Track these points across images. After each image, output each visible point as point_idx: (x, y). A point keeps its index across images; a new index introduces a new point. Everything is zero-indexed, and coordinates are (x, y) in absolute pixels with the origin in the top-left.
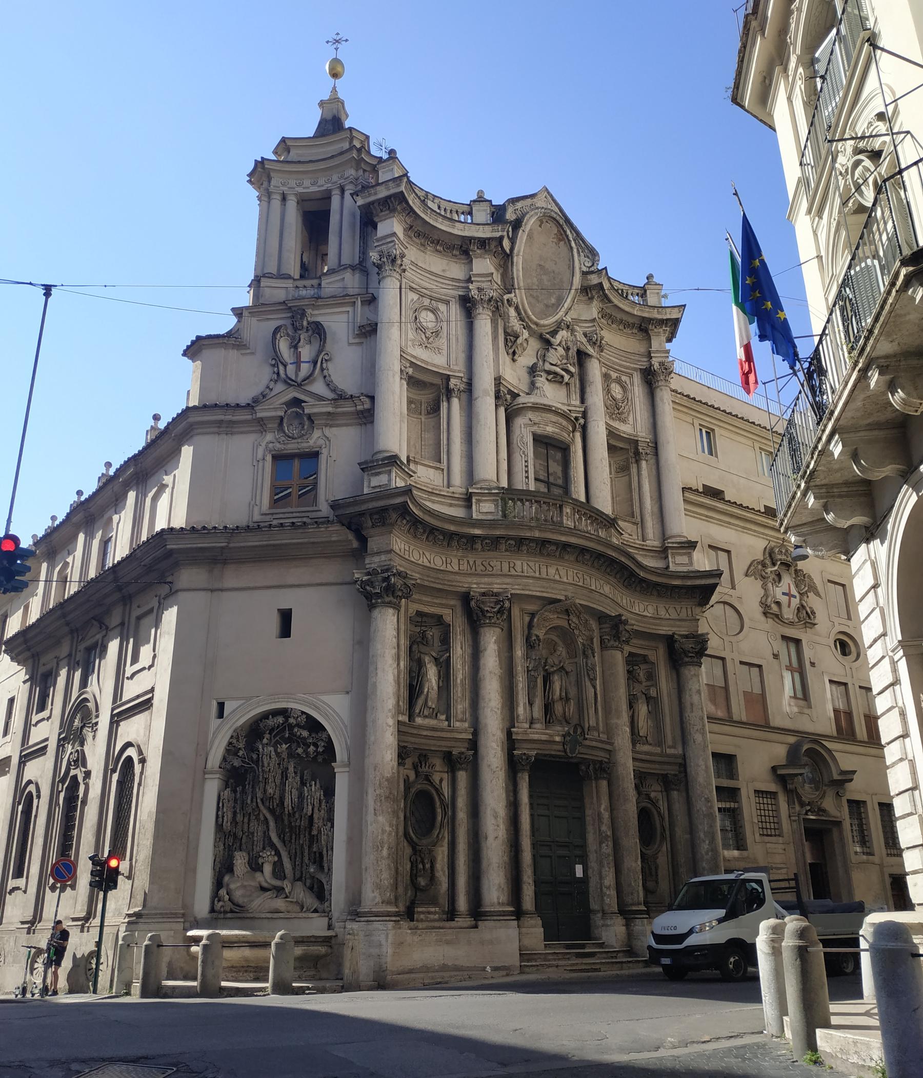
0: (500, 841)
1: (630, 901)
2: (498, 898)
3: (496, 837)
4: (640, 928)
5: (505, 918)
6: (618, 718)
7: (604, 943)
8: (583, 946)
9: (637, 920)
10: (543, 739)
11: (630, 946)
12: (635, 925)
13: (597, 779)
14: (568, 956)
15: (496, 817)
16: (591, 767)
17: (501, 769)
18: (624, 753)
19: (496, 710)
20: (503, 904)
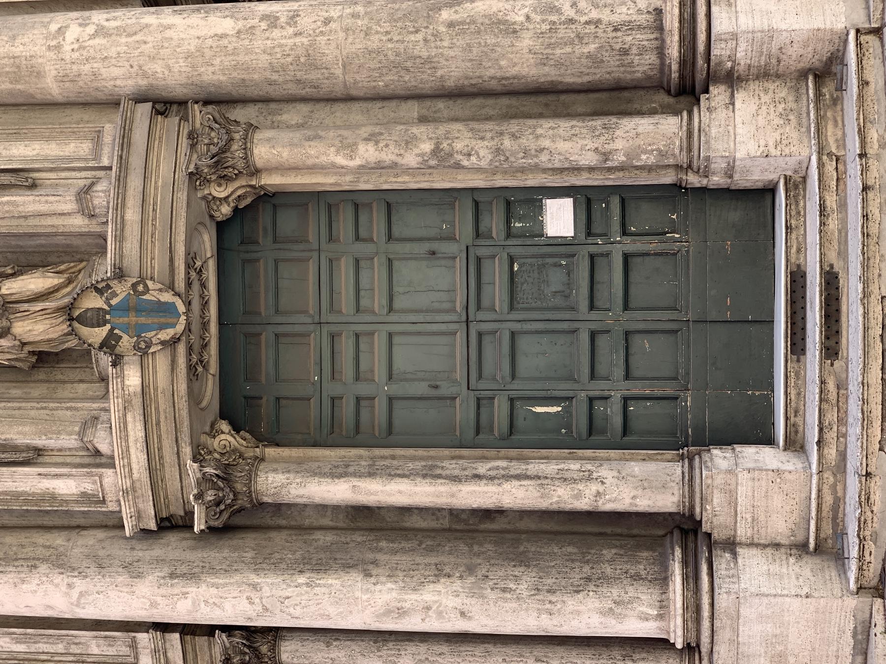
0: (473, 605)
1: (651, 58)
2: (646, 618)
3: (463, 614)
4: (742, 46)
5: (706, 613)
6: (39, 75)
7: (787, 180)
8: (797, 279)
9: (715, 52)
10: (141, 434)
11: (803, 75)
12: (732, 58)
13: (256, 172)
14: (831, 386)
15: (402, 613)
16: (220, 192)
17: (255, 587)
18: (152, 58)
19: (75, 594)
20: (663, 606)
